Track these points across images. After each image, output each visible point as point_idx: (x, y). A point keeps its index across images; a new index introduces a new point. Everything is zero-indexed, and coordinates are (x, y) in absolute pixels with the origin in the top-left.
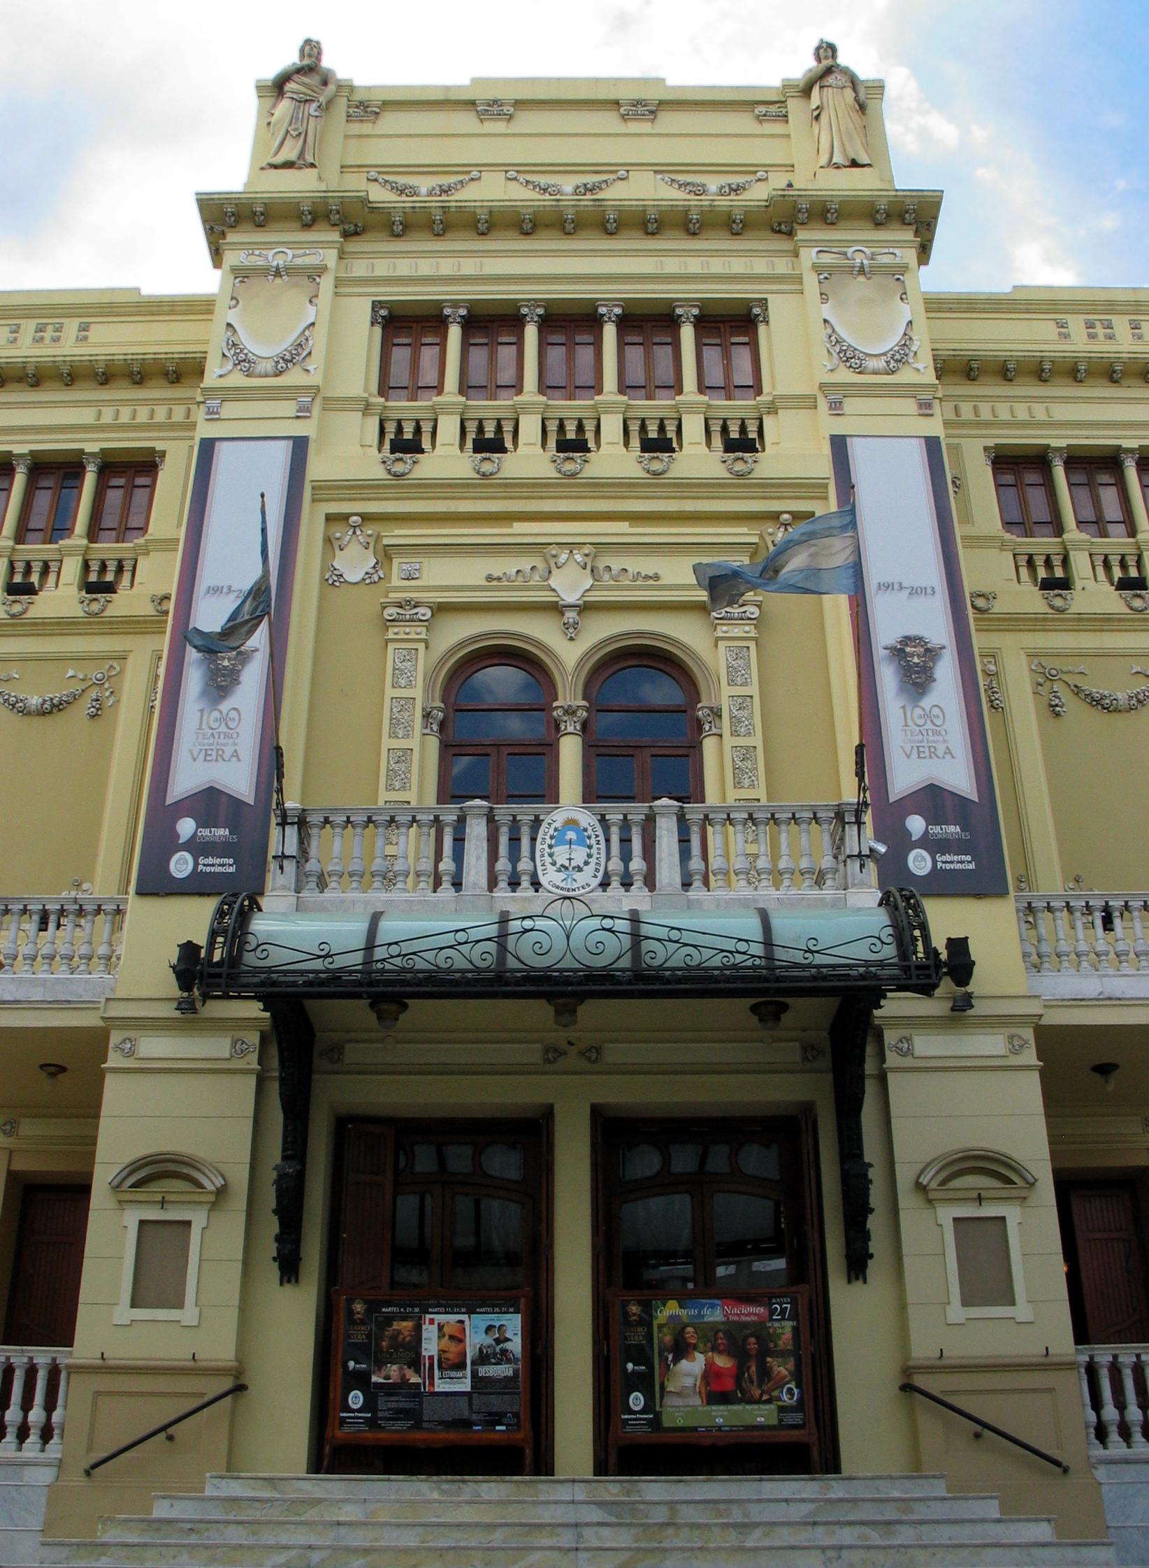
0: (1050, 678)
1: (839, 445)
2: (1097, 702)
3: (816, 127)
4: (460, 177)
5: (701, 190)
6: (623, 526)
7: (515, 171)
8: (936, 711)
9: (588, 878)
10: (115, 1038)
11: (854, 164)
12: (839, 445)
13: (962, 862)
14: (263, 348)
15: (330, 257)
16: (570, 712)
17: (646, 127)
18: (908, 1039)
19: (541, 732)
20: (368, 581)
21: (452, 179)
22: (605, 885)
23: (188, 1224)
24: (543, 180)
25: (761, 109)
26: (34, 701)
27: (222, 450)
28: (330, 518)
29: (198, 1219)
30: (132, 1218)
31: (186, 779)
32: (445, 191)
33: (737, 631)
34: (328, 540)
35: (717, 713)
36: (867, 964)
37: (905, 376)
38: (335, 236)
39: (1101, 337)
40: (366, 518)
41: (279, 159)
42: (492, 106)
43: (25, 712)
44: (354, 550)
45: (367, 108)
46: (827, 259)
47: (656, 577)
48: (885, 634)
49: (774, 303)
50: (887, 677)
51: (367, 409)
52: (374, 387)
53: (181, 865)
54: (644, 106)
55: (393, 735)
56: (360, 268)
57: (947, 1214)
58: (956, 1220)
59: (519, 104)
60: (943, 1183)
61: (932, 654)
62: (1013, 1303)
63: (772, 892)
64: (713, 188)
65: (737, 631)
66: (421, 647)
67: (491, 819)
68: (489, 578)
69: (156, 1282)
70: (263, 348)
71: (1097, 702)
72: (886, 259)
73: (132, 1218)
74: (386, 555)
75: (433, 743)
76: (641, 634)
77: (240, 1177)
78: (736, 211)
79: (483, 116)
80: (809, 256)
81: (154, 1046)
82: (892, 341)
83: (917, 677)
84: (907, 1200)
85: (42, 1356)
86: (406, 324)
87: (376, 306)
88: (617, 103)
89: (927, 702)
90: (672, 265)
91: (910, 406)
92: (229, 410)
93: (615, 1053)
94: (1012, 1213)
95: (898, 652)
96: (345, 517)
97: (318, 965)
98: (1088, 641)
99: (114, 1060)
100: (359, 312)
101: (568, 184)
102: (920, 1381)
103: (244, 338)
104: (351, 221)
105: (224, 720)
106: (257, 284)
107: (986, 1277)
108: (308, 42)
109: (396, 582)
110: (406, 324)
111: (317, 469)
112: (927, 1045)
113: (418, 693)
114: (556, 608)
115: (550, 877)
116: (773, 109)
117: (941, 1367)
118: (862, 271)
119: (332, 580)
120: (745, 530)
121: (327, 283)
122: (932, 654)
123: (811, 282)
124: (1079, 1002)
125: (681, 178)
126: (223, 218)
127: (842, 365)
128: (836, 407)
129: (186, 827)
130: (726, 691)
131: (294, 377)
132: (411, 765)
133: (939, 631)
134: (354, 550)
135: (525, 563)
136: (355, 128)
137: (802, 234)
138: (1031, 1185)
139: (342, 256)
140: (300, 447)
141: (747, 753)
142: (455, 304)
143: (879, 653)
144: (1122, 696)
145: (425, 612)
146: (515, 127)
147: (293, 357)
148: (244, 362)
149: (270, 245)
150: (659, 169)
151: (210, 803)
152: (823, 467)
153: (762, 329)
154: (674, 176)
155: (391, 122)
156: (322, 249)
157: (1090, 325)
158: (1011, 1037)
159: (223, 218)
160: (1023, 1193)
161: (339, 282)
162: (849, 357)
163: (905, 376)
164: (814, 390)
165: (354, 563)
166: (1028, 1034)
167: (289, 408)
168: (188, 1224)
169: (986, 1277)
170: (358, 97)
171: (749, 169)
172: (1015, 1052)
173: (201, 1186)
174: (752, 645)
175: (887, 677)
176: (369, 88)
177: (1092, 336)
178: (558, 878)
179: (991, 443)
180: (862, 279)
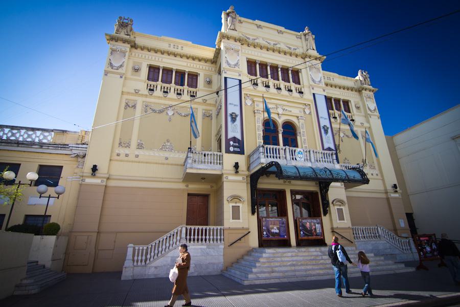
3: (307, 42)
5: (290, 48)
9: (303, 159)
10: (224, 176)
14: (232, 63)
22: (305, 161)
24: (269, 42)
26: (183, 114)
30: (231, 205)
31: (230, 136)
32: (254, 40)
35: (300, 133)
37: (320, 85)
41: (231, 28)
43: (182, 116)
53: (232, 149)
57: (336, 207)
62: (344, 220)
67: (289, 149)
69: (236, 214)
70: (232, 63)
73: (231, 205)
74: (253, 102)
81: (231, 178)
82: (319, 79)
84: (331, 205)
85: (219, 227)
89: (328, 135)
91: (322, 90)
99: (225, 179)
101: (272, 43)
102: (335, 230)
105: (235, 126)
107: (341, 217)
114: (278, 114)
115: (298, 159)
117: (337, 228)
122: (328, 128)
129: (232, 143)
130: (302, 130)
131: (237, 68)
141: (305, 139)
147: (237, 65)
148: (229, 64)
150: (285, 43)
151: (234, 139)
153: (300, 74)
156: (237, 45)
168: (239, 206)
169: (341, 217)
173: (241, 201)
178: (299, 159)
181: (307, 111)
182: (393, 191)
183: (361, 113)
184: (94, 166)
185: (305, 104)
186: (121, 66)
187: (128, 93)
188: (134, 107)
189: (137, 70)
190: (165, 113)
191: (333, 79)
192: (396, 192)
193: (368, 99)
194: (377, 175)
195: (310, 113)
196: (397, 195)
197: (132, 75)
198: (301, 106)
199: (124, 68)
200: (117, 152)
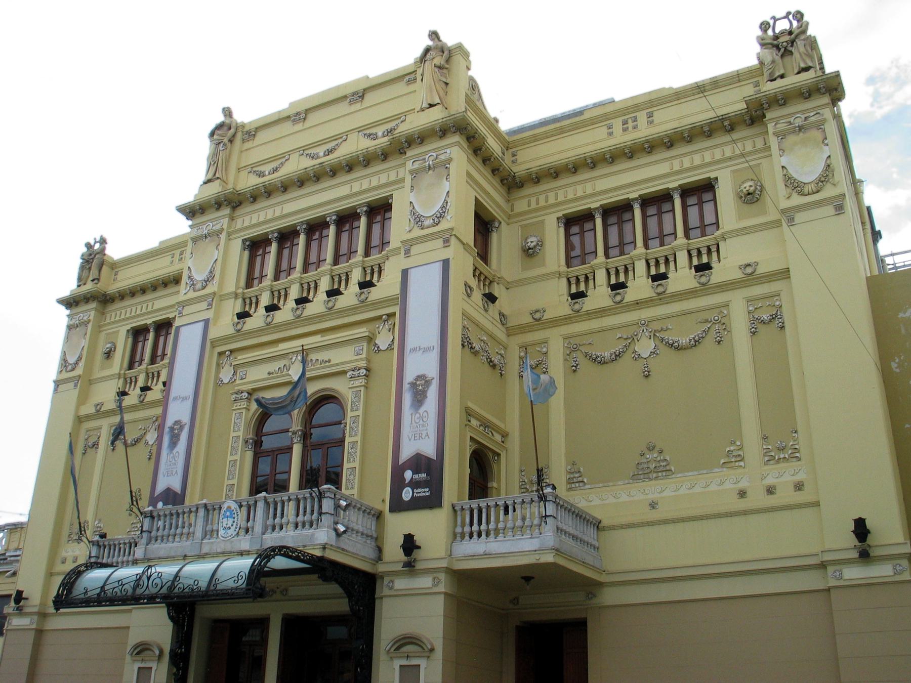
0: (575, 350)
1: (405, 273)
2: (595, 360)
4: (280, 161)
6: (317, 338)
7: (303, 150)
8: (425, 414)
9: (232, 531)
11: (431, 106)
12: (405, 273)
13: (424, 492)
15: (226, 221)
16: (294, 433)
17: (358, 106)
18: (392, 582)
19: (287, 443)
20: (232, 381)
21: (280, 161)
23: (151, 668)
25: (407, 78)
27: (183, 330)
28: (221, 354)
29: (154, 665)
32: (275, 170)
33: (357, 383)
34: (218, 365)
36: (232, 589)
38: (227, 211)
39: (630, 129)
40: (231, 351)
42: (299, 115)
44: (227, 367)
45: (250, 133)
46: (416, 165)
47: (329, 361)
48: (409, 377)
49: (395, 194)
50: (407, 398)
51: (236, 296)
52: (243, 282)
54: (359, 94)
55: (232, 455)
56: (239, 224)
57: (397, 663)
58: (401, 666)
59: (307, 111)
60: (398, 649)
61: (428, 383)
63: (292, 533)
64: (380, 134)
65: (357, 383)
66: (244, 411)
68: (269, 374)
70: (199, 277)
71: (595, 360)
72: (442, 157)
73: (137, 665)
74: (236, 368)
75: (249, 455)
76: (319, 391)
77: (167, 649)
78: (378, 150)
79: (295, 122)
80: (409, 165)
83: (419, 398)
86: (256, 246)
87: (244, 241)
88: (345, 97)
89: (421, 410)
90: (356, 187)
91: (439, 243)
92: (187, 310)
93: (293, 592)
94: (423, 663)
95: (413, 385)
96: (225, 352)
97: (82, 596)
98: (595, 324)
100: (237, 245)
101: (321, 151)
103: (194, 273)
104: (232, 202)
106: (201, 243)
108: (224, 109)
109: (238, 382)
110: (256, 246)
111: (213, 334)
112: (401, 584)
113: (241, 434)
116: (412, 76)
118: (429, 168)
119: (219, 384)
120: (364, 329)
121: (223, 236)
123: (408, 179)
124: (473, 557)
125: (368, 132)
126: (191, 211)
127: (416, 226)
128: (407, 252)
131: (209, 290)
132: (238, 464)
133: (433, 372)
134: (227, 367)
135: (280, 364)
136: (248, 145)
137: (410, 153)
138: (432, 650)
139: (232, 219)
140: (207, 322)
142: (273, 232)
143: (406, 386)
144: (607, 354)
145: (245, 395)
146: (308, 123)
149: (204, 223)
150: (359, 130)
152: (396, 290)
154: (365, 132)
155: (261, 137)
157: (625, 123)
158: (434, 579)
159: (191, 211)
160: (427, 654)
161: (229, 234)
162: (418, 220)
163: (444, 225)
164: (400, 245)
165: (226, 375)
166: (442, 576)
167: (204, 305)
168: (151, 668)
170: (247, 129)
171: (396, 117)
172: (436, 585)
174: (362, 389)
175: (407, 398)
176: (250, 123)
177: (625, 130)
179: (560, 214)
180: (431, 172)
181: (383, 341)
182: (855, 554)
183: (764, 212)
184: (405, 536)
185: (380, 317)
186: (80, 359)
187: (88, 417)
188: (95, 445)
189: (109, 354)
190: (143, 441)
191: (650, 115)
192: (865, 556)
193: (792, 139)
194: (799, 486)
195: (390, 347)
196: (881, 571)
197: (103, 368)
198: (362, 331)
199: (82, 364)
200: (64, 554)
